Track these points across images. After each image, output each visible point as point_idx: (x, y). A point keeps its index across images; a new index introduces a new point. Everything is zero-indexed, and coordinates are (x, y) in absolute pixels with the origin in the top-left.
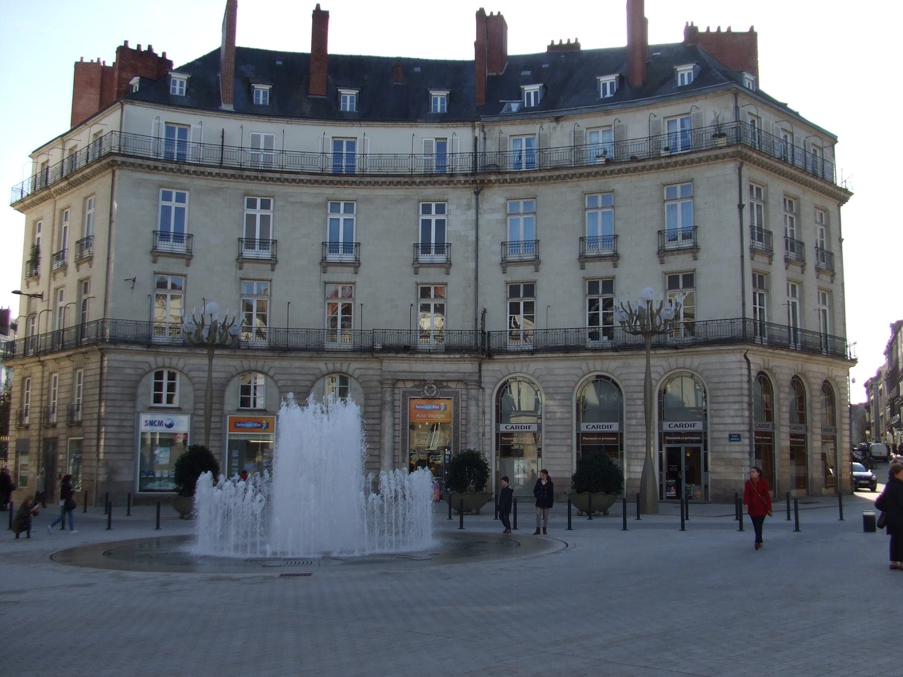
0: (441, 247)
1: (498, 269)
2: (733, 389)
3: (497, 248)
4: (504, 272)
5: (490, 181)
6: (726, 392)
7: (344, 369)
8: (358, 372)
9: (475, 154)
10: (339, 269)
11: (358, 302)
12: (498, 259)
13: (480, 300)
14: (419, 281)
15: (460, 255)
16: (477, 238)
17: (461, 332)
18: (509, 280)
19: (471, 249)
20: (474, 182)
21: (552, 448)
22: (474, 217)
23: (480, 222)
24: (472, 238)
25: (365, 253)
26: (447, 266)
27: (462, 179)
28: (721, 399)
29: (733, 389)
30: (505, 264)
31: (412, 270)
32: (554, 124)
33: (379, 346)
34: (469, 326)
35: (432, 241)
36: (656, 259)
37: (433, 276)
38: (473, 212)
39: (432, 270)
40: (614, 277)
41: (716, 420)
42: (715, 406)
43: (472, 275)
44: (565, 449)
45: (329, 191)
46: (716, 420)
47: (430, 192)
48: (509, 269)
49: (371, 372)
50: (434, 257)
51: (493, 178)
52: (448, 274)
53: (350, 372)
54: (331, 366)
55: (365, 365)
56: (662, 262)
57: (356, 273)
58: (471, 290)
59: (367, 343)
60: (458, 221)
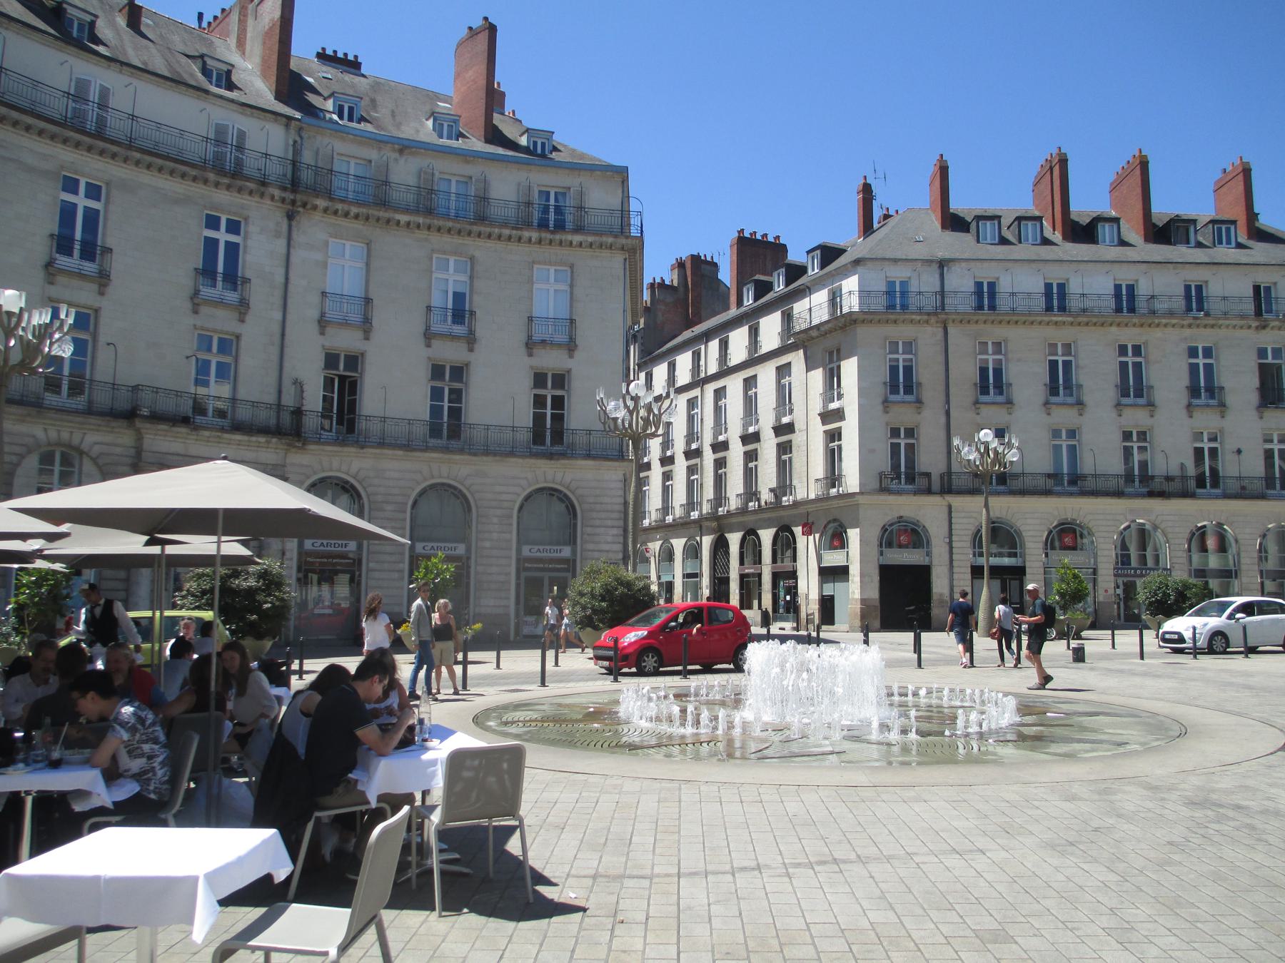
0: (232, 278)
1: (314, 328)
2: (612, 511)
3: (316, 299)
4: (322, 333)
5: (315, 208)
6: (603, 515)
7: (76, 441)
8: (96, 450)
9: (294, 163)
10: (76, 282)
11: (103, 339)
12: (315, 314)
13: (287, 365)
14: (199, 323)
15: (262, 296)
16: (287, 279)
17: (254, 404)
18: (327, 344)
19: (278, 293)
20: (293, 202)
21: (377, 575)
22: (284, 251)
23: (293, 259)
24: (280, 279)
25: (118, 264)
26: (243, 307)
27: (277, 193)
28: (597, 522)
29: (612, 511)
30: (323, 323)
31: (189, 305)
32: (396, 155)
33: (145, 412)
34: (271, 398)
35: (220, 269)
36: (523, 350)
37: (222, 321)
38: (283, 242)
39: (221, 313)
40: (467, 365)
41: (590, 546)
42: (589, 530)
43: (276, 329)
44: (396, 575)
45: (66, 155)
46: (590, 546)
47: (223, 197)
48: (329, 330)
49: (118, 450)
50: (219, 290)
51: (321, 203)
52: (242, 321)
53: (85, 447)
54: (53, 435)
55: (108, 438)
56: (530, 355)
57: (102, 294)
58: (275, 350)
59: (123, 404)
60: (260, 251)
